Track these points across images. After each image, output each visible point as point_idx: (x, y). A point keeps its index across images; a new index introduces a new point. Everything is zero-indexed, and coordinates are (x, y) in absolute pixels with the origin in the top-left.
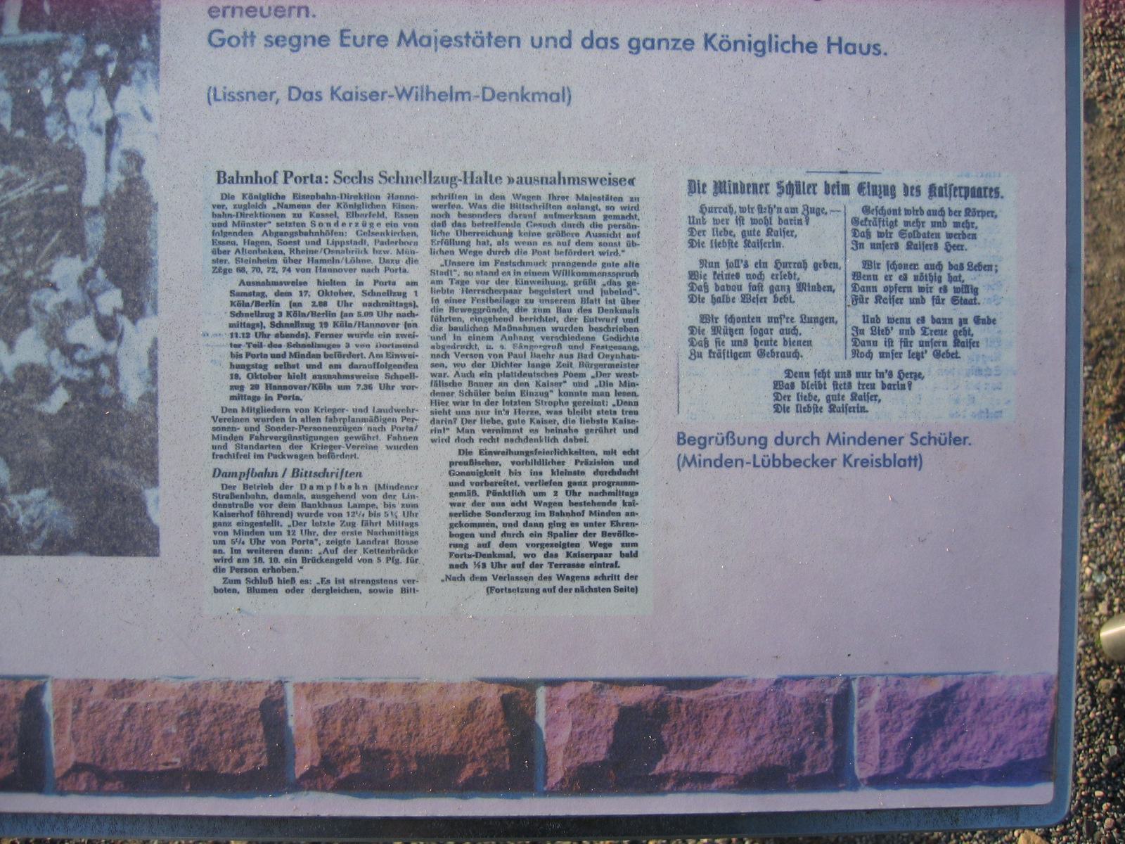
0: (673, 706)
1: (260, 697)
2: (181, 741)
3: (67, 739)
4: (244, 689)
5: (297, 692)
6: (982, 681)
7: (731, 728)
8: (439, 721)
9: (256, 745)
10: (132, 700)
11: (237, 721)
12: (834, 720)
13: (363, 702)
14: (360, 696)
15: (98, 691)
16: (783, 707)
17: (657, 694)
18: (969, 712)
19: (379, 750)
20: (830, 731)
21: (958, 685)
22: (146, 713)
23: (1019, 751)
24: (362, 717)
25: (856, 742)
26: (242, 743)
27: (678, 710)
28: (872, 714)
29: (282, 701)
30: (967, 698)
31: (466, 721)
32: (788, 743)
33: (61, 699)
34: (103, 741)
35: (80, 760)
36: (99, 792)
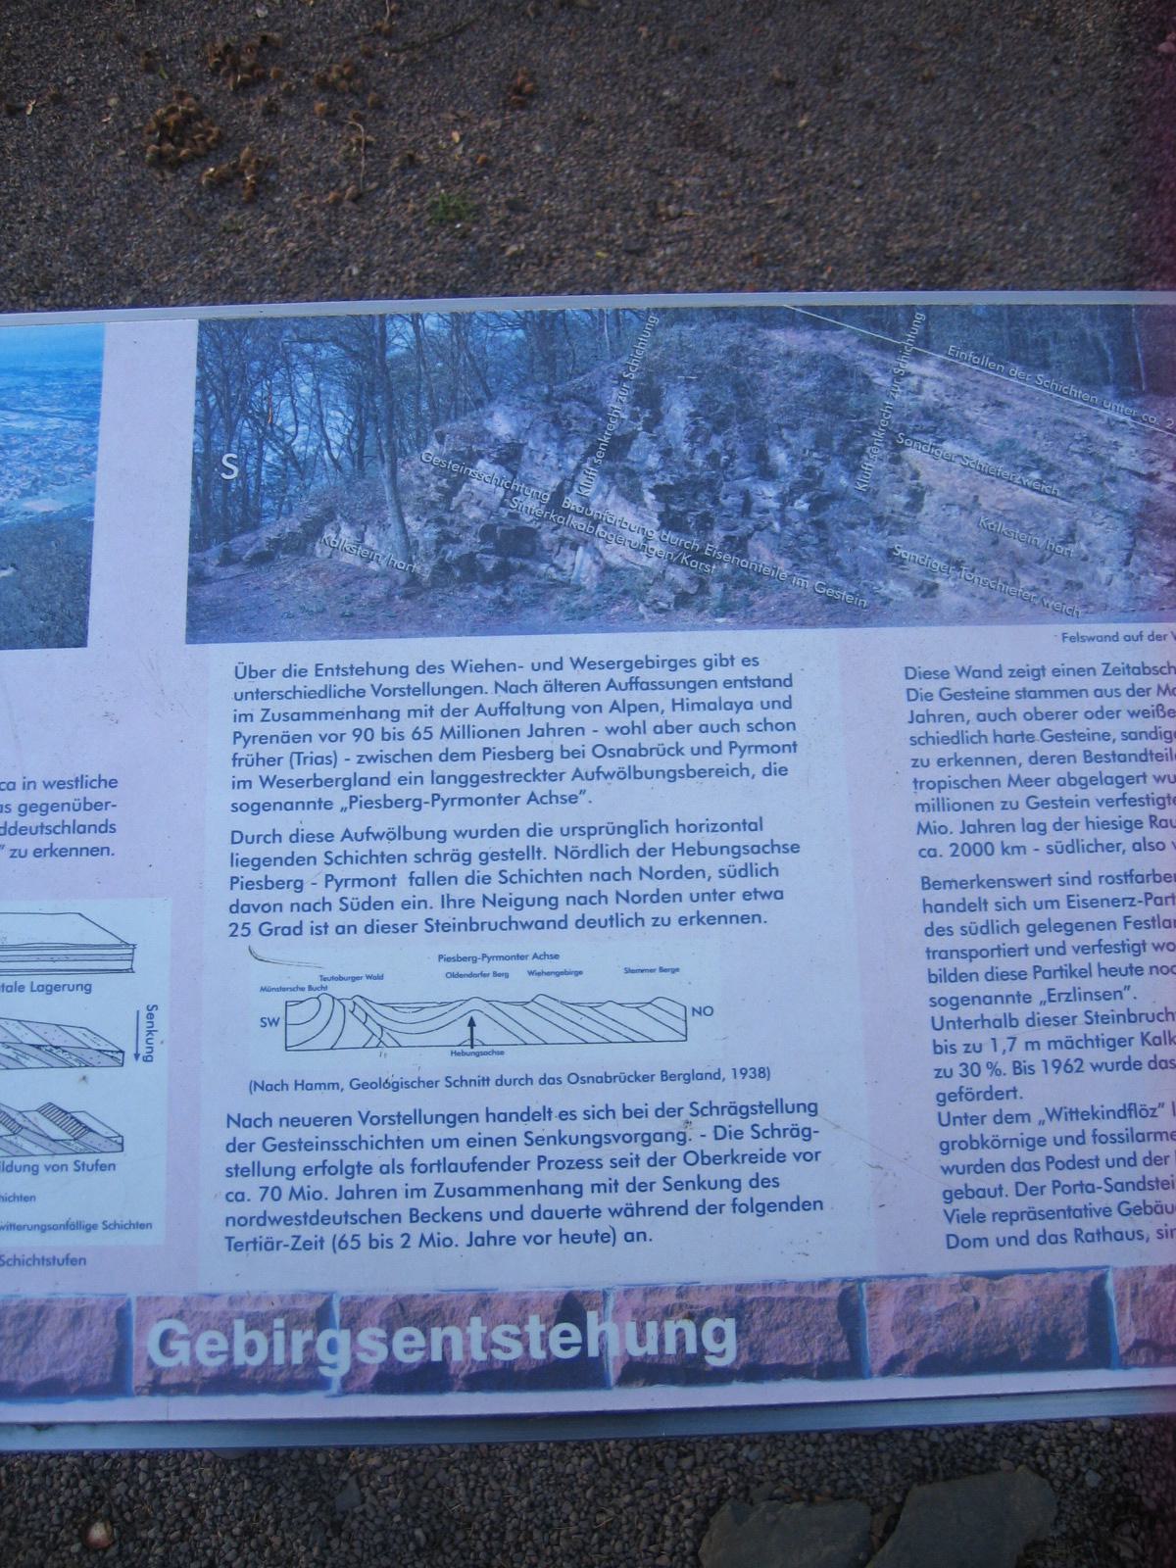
3: (1128, 1318)
15: (1151, 1277)
35: (1140, 1336)
36: (1154, 1363)
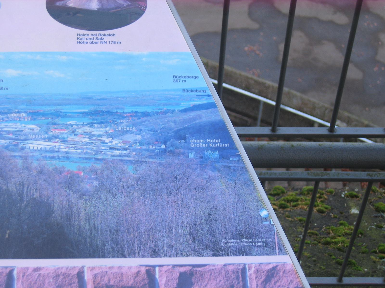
0: (195, 272)
1: (76, 271)
2: (54, 283)
3: (20, 284)
4: (72, 269)
5: (87, 269)
6: (284, 265)
7: (212, 278)
8: (128, 277)
9: (75, 285)
10: (40, 272)
11: (70, 278)
12: (241, 275)
13: (107, 272)
14: (106, 270)
15: (30, 271)
16: (227, 272)
17: (190, 268)
18: (281, 273)
19: (111, 285)
20: (241, 279)
21: (277, 266)
22: (44, 276)
23: (297, 284)
24: (106, 276)
25: (249, 282)
26: (71, 284)
27: (196, 273)
28: (253, 274)
29: (83, 272)
30: (280, 269)
31: (135, 277)
32: (229, 282)
33: (19, 273)
34: (30, 284)
